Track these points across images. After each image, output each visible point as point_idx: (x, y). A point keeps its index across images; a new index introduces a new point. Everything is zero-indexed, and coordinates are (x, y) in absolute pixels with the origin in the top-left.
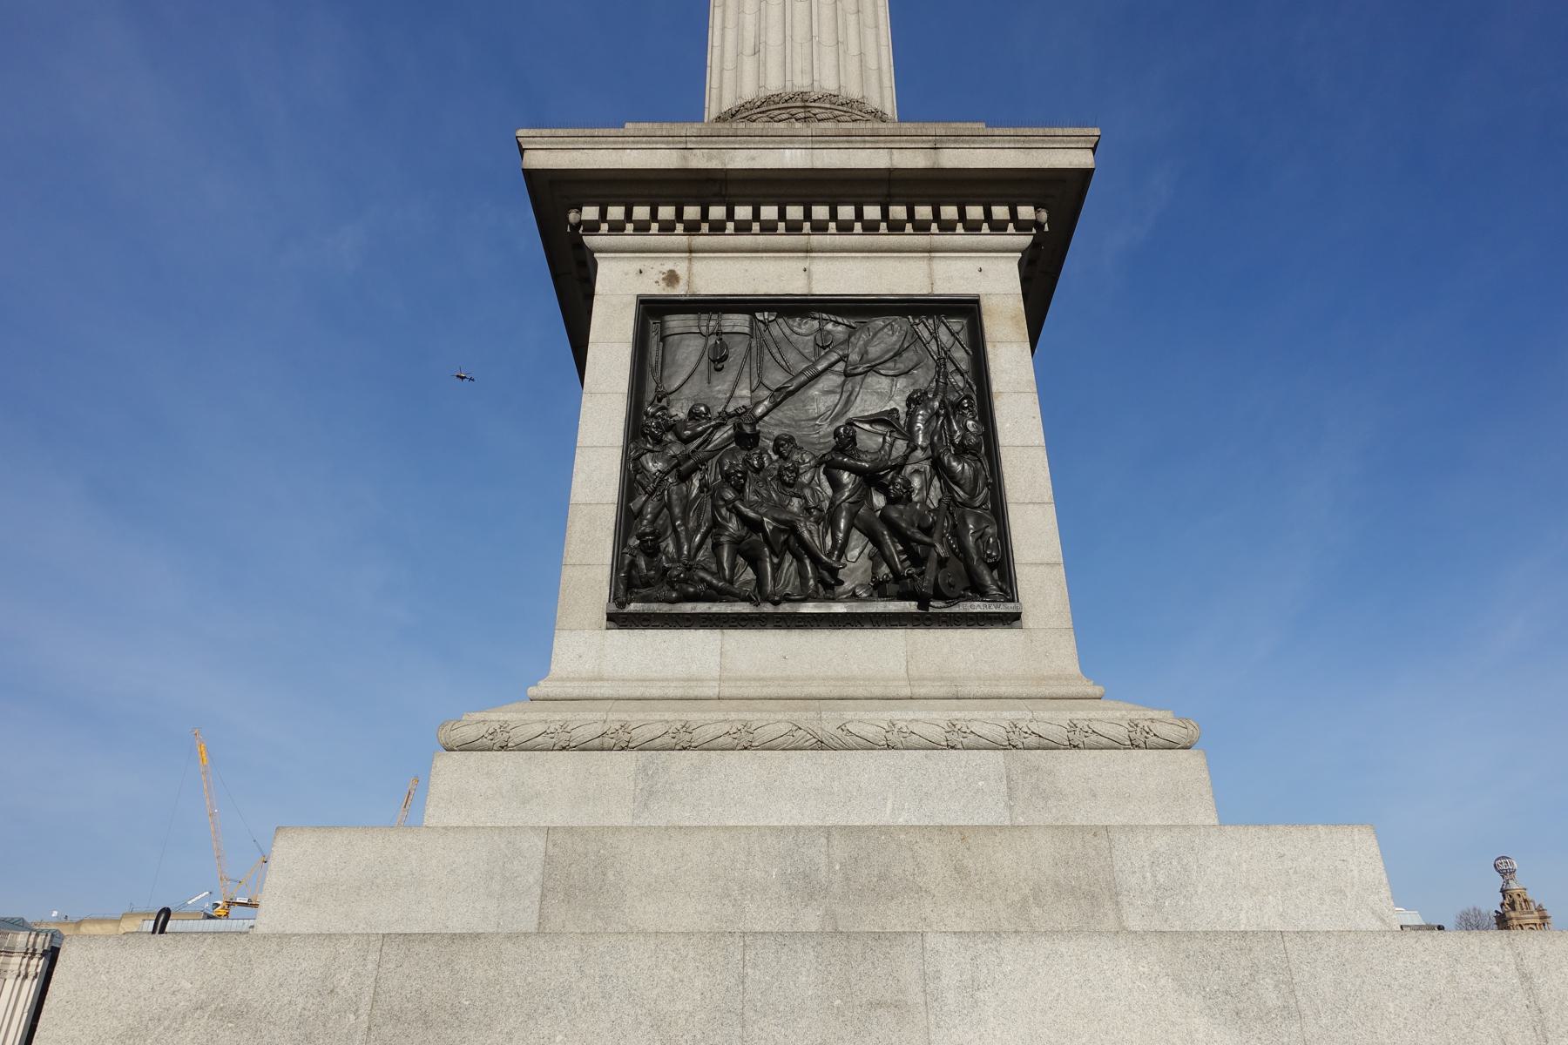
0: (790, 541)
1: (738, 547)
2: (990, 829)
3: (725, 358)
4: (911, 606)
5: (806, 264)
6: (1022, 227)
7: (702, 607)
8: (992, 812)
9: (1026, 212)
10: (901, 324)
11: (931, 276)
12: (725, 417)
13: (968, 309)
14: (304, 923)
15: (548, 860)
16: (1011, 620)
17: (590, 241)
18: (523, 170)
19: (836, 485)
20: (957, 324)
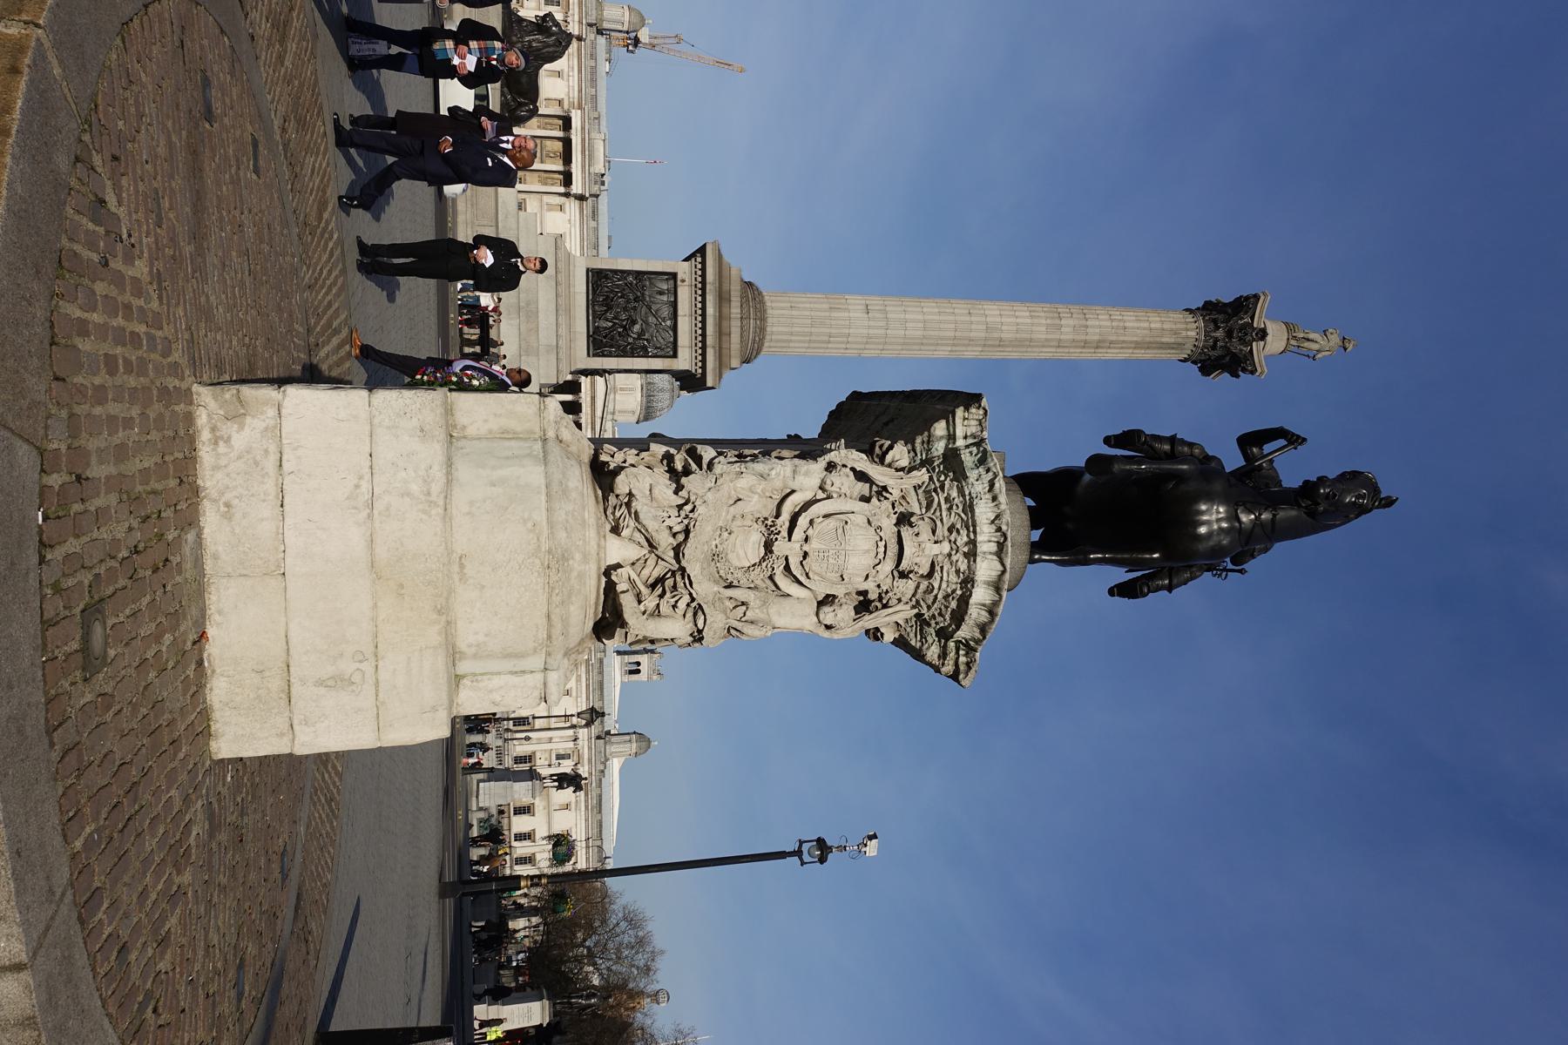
0: (609, 308)
1: (608, 297)
2: (538, 339)
3: (661, 294)
4: (591, 333)
6: (696, 370)
7: (590, 288)
8: (543, 341)
9: (700, 371)
10: (672, 339)
12: (643, 294)
13: (675, 356)
14: (521, 220)
16: (588, 355)
20: (671, 353)
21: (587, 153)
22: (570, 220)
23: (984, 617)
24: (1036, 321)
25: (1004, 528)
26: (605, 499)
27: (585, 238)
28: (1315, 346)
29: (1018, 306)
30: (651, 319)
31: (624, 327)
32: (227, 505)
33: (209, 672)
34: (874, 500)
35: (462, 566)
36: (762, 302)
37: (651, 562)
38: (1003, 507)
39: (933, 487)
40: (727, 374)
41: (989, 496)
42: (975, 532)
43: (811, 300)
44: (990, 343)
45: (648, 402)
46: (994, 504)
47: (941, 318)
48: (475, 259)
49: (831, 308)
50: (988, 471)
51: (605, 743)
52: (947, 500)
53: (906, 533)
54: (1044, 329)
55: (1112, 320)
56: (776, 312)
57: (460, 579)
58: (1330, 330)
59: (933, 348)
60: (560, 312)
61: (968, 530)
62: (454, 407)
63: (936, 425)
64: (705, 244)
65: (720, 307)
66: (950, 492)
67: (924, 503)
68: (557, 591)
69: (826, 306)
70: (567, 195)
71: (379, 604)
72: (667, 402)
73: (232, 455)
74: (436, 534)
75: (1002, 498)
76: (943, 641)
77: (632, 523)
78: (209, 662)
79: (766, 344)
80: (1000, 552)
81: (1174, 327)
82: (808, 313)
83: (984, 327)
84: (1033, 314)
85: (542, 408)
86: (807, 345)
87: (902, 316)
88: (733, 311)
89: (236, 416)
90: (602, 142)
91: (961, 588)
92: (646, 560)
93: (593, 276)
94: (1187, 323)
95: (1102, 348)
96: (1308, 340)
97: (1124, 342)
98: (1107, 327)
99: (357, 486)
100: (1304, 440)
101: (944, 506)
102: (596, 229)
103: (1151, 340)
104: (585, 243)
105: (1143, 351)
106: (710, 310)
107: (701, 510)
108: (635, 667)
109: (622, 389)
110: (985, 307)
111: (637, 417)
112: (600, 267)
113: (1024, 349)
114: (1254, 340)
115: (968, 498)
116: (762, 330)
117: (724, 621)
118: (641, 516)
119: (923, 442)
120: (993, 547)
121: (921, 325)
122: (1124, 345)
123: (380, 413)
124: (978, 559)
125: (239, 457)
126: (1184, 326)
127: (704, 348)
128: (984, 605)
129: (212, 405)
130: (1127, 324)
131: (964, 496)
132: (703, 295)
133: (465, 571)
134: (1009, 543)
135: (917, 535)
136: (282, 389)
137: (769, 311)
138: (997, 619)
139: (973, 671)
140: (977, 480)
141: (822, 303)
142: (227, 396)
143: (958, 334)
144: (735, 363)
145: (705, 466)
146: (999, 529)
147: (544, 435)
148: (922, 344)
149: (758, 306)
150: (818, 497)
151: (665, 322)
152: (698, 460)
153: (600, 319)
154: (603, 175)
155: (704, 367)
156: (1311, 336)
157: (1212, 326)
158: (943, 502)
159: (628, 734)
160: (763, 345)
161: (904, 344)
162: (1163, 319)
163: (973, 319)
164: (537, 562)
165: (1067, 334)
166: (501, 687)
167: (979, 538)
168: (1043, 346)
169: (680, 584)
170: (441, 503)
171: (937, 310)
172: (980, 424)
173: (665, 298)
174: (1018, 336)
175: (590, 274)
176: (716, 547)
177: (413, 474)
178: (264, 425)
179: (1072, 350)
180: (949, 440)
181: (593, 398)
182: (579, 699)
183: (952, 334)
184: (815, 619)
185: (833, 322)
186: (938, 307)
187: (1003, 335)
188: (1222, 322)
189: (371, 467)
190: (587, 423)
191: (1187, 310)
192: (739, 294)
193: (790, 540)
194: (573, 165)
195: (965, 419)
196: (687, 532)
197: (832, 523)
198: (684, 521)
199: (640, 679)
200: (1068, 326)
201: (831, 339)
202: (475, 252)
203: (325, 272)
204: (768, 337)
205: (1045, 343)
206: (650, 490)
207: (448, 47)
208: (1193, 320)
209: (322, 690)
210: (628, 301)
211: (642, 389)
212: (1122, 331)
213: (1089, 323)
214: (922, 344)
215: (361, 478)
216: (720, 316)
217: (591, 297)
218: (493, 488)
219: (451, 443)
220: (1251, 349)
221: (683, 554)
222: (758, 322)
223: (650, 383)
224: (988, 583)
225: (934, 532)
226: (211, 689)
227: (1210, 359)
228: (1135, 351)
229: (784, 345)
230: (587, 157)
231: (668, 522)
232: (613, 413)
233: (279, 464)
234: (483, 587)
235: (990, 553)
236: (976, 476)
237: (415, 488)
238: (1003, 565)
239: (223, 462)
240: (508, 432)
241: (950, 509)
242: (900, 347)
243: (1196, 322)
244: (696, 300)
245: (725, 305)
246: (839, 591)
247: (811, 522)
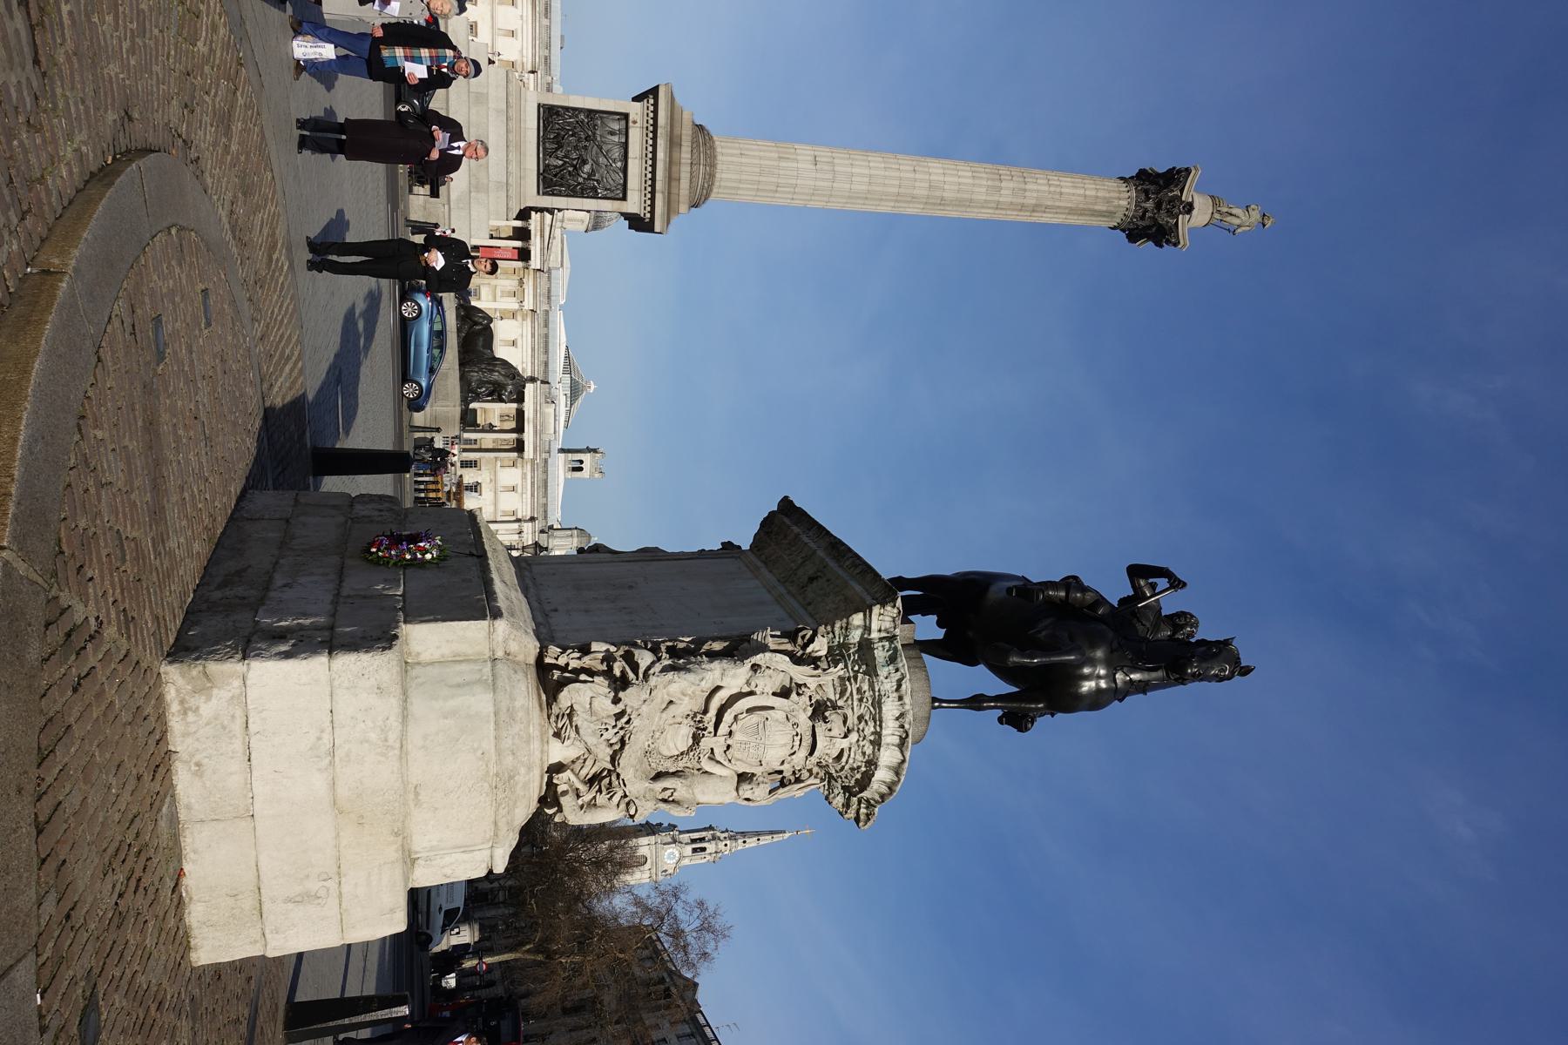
0: (560, 146)
1: (558, 134)
3: (612, 135)
4: (541, 171)
5: (638, 156)
7: (541, 124)
8: (493, 177)
9: (648, 215)
10: (622, 181)
11: (634, 190)
12: (594, 134)
13: (624, 198)
15: (482, 94)
17: (645, 101)
18: (658, 86)
19: (575, 159)
20: (621, 195)
23: (884, 789)
24: (977, 182)
25: (907, 726)
26: (549, 705)
27: (537, 35)
28: (1236, 221)
29: (962, 166)
30: (602, 160)
31: (575, 167)
32: (198, 764)
33: (187, 900)
34: (794, 695)
35: (417, 794)
36: (713, 148)
37: (589, 763)
38: (907, 707)
39: (847, 675)
40: (675, 220)
41: (896, 695)
42: (881, 726)
43: (760, 147)
44: (931, 201)
46: (900, 703)
47: (887, 173)
48: (426, 262)
49: (780, 158)
50: (897, 670)
51: (548, 537)
52: (859, 690)
53: (821, 728)
54: (984, 190)
55: (1050, 185)
56: (725, 158)
57: (416, 805)
58: (1253, 206)
59: (878, 203)
60: (511, 148)
61: (875, 722)
62: (408, 638)
63: (854, 616)
64: (658, 86)
65: (670, 152)
66: (862, 685)
67: (839, 689)
68: (503, 806)
69: (776, 155)
71: (341, 834)
73: (201, 722)
74: (393, 772)
75: (907, 700)
76: (847, 794)
77: (573, 734)
78: (187, 892)
79: (715, 190)
80: (902, 745)
81: (1107, 195)
82: (757, 161)
83: (927, 185)
84: (974, 174)
85: (492, 630)
86: (754, 193)
87: (849, 170)
88: (683, 155)
89: (206, 686)
91: (866, 766)
92: (585, 760)
93: (544, 112)
94: (1120, 192)
95: (1037, 211)
96: (1231, 214)
97: (1059, 207)
98: (1045, 191)
99: (319, 739)
100: (1185, 584)
101: (856, 697)
102: (549, 28)
103: (1085, 207)
104: (537, 42)
105: (1076, 218)
106: (661, 155)
107: (636, 722)
108: (578, 465)
110: (930, 164)
112: (551, 103)
113: (964, 209)
114: (1180, 213)
115: (877, 694)
116: (711, 176)
117: (654, 808)
118: (581, 731)
119: (842, 628)
120: (896, 740)
121: (867, 180)
122: (1058, 211)
123: (340, 676)
124: (882, 749)
125: (207, 724)
126: (1117, 195)
127: (653, 193)
128: (884, 782)
129: (180, 682)
130: (1063, 190)
131: (874, 690)
132: (655, 139)
133: (420, 798)
134: (910, 740)
135: (830, 730)
136: (246, 662)
137: (719, 157)
138: (895, 794)
139: (872, 821)
140: (886, 678)
141: (771, 152)
142: (194, 672)
143: (902, 191)
144: (683, 208)
145: (641, 675)
146: (902, 726)
147: (493, 655)
148: (866, 198)
149: (708, 152)
150: (743, 691)
151: (615, 163)
152: (635, 667)
153: (550, 157)
155: (652, 212)
156: (1234, 211)
157: (1143, 197)
158: (855, 692)
159: (570, 529)
160: (711, 190)
161: (849, 197)
162: (1098, 187)
163: (917, 176)
164: (486, 785)
165: (1006, 196)
166: (451, 864)
167: (884, 732)
168: (983, 207)
169: (615, 782)
170: (398, 745)
171: (883, 165)
172: (894, 621)
173: (616, 139)
174: (959, 195)
175: (541, 109)
176: (649, 746)
177: (372, 725)
178: (230, 694)
179: (1009, 212)
180: (865, 630)
182: (524, 496)
183: (895, 190)
184: (735, 793)
185: (781, 172)
186: (885, 162)
187: (945, 194)
188: (1153, 193)
189: (332, 721)
190: (536, 230)
191: (1121, 178)
192: (690, 138)
193: (715, 735)
195: (880, 614)
196: (623, 742)
197: (755, 718)
198: (620, 732)
199: (582, 476)
200: (1007, 188)
201: (779, 189)
202: (426, 255)
203: (276, 310)
204: (717, 184)
205: (984, 205)
206: (590, 704)
207: (397, 55)
208: (1126, 189)
209: (291, 906)
210: (579, 140)
212: (1057, 197)
213: (1028, 187)
214: (866, 198)
215: (322, 731)
216: (670, 162)
217: (541, 134)
218: (445, 721)
219: (406, 672)
220: (1177, 221)
221: (619, 764)
222: (708, 168)
224: (889, 768)
225: (845, 722)
226: (189, 913)
227: (1137, 228)
228: (1069, 217)
229: (733, 192)
231: (607, 735)
232: (562, 221)
233: (245, 726)
234: (436, 809)
235: (893, 745)
236: (885, 674)
237: (373, 736)
238: (903, 756)
239: (193, 728)
240: (460, 656)
241: (861, 700)
242: (845, 201)
243: (1128, 191)
244: (647, 143)
245: (676, 149)
246: (758, 771)
247: (736, 718)
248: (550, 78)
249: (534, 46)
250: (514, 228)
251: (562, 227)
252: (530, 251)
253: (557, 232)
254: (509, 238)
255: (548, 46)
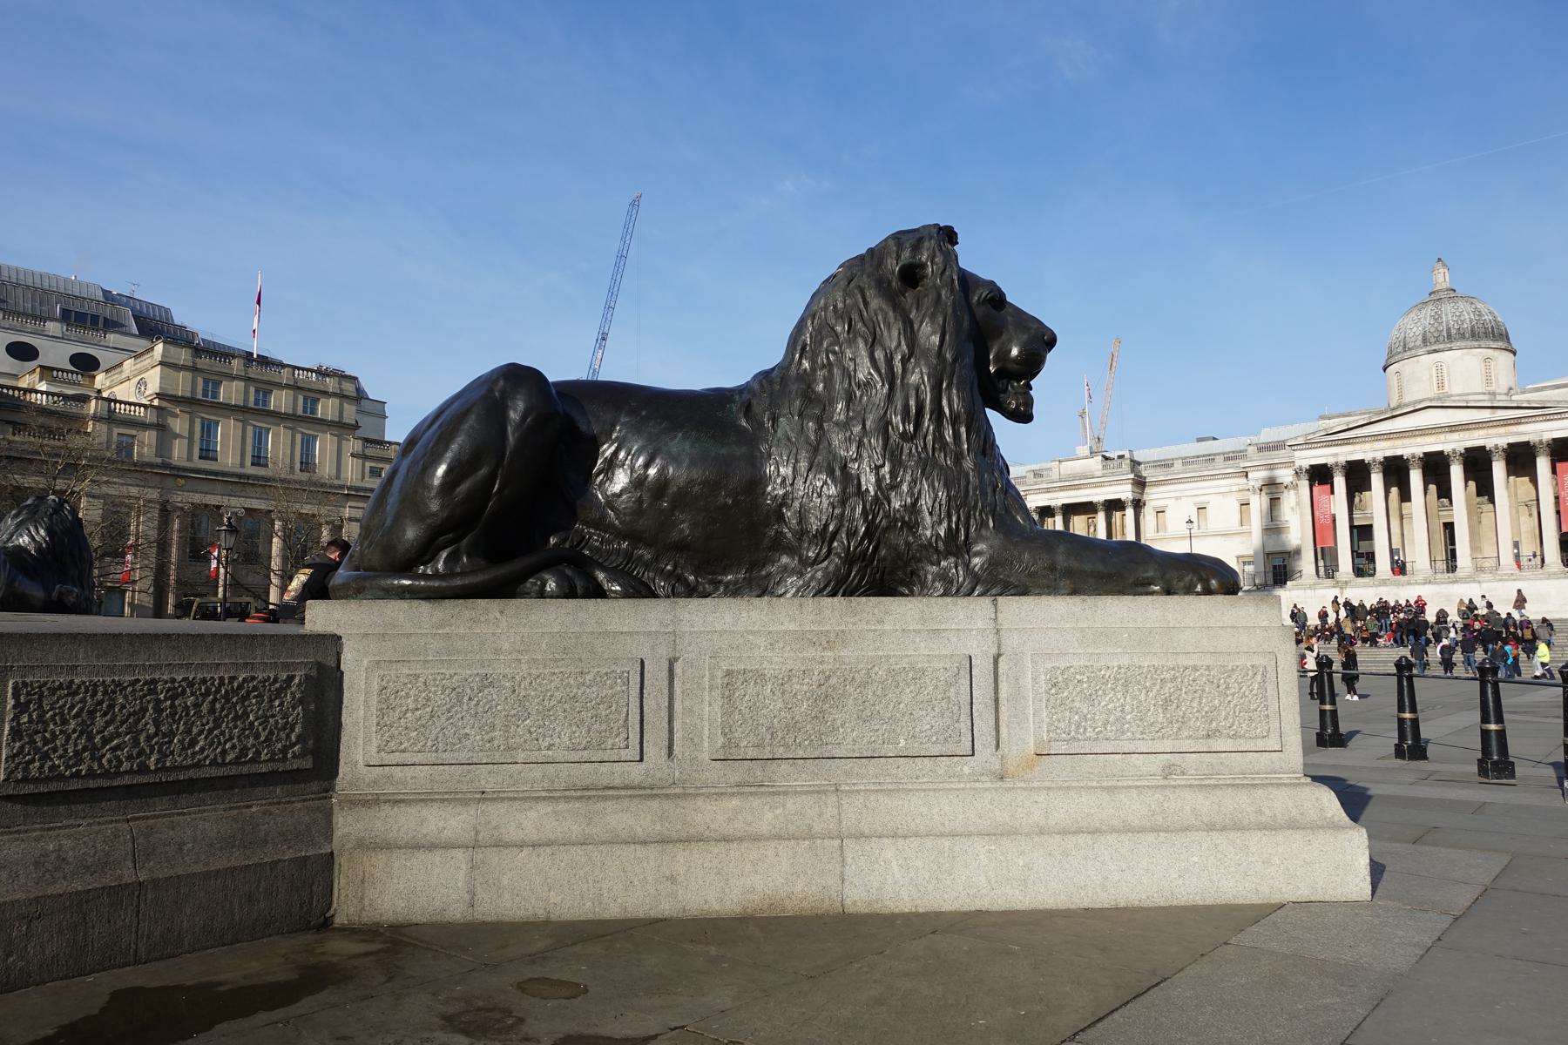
21: (1077, 482)
22: (1177, 498)
45: (1462, 336)
70: (1138, 505)
72: (1461, 305)
90: (1063, 463)
102: (1186, 461)
104: (1206, 473)
109: (1441, 385)
111: (1497, 353)
154: (1106, 458)
181: (1452, 428)
190: (1506, 435)
194: (1095, 499)
211: (1436, 351)
223: (1425, 341)
230: (1082, 482)
232: (1494, 394)
248: (1251, 449)
249: (1213, 477)
250: (1509, 473)
251: (1507, 394)
252: (1554, 440)
253: (1518, 398)
254: (1534, 481)
255: (1210, 458)
